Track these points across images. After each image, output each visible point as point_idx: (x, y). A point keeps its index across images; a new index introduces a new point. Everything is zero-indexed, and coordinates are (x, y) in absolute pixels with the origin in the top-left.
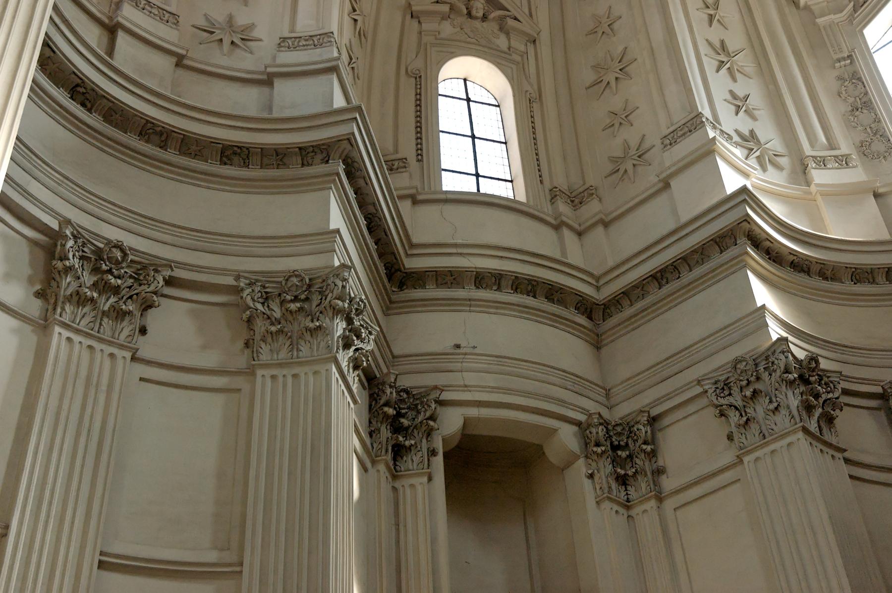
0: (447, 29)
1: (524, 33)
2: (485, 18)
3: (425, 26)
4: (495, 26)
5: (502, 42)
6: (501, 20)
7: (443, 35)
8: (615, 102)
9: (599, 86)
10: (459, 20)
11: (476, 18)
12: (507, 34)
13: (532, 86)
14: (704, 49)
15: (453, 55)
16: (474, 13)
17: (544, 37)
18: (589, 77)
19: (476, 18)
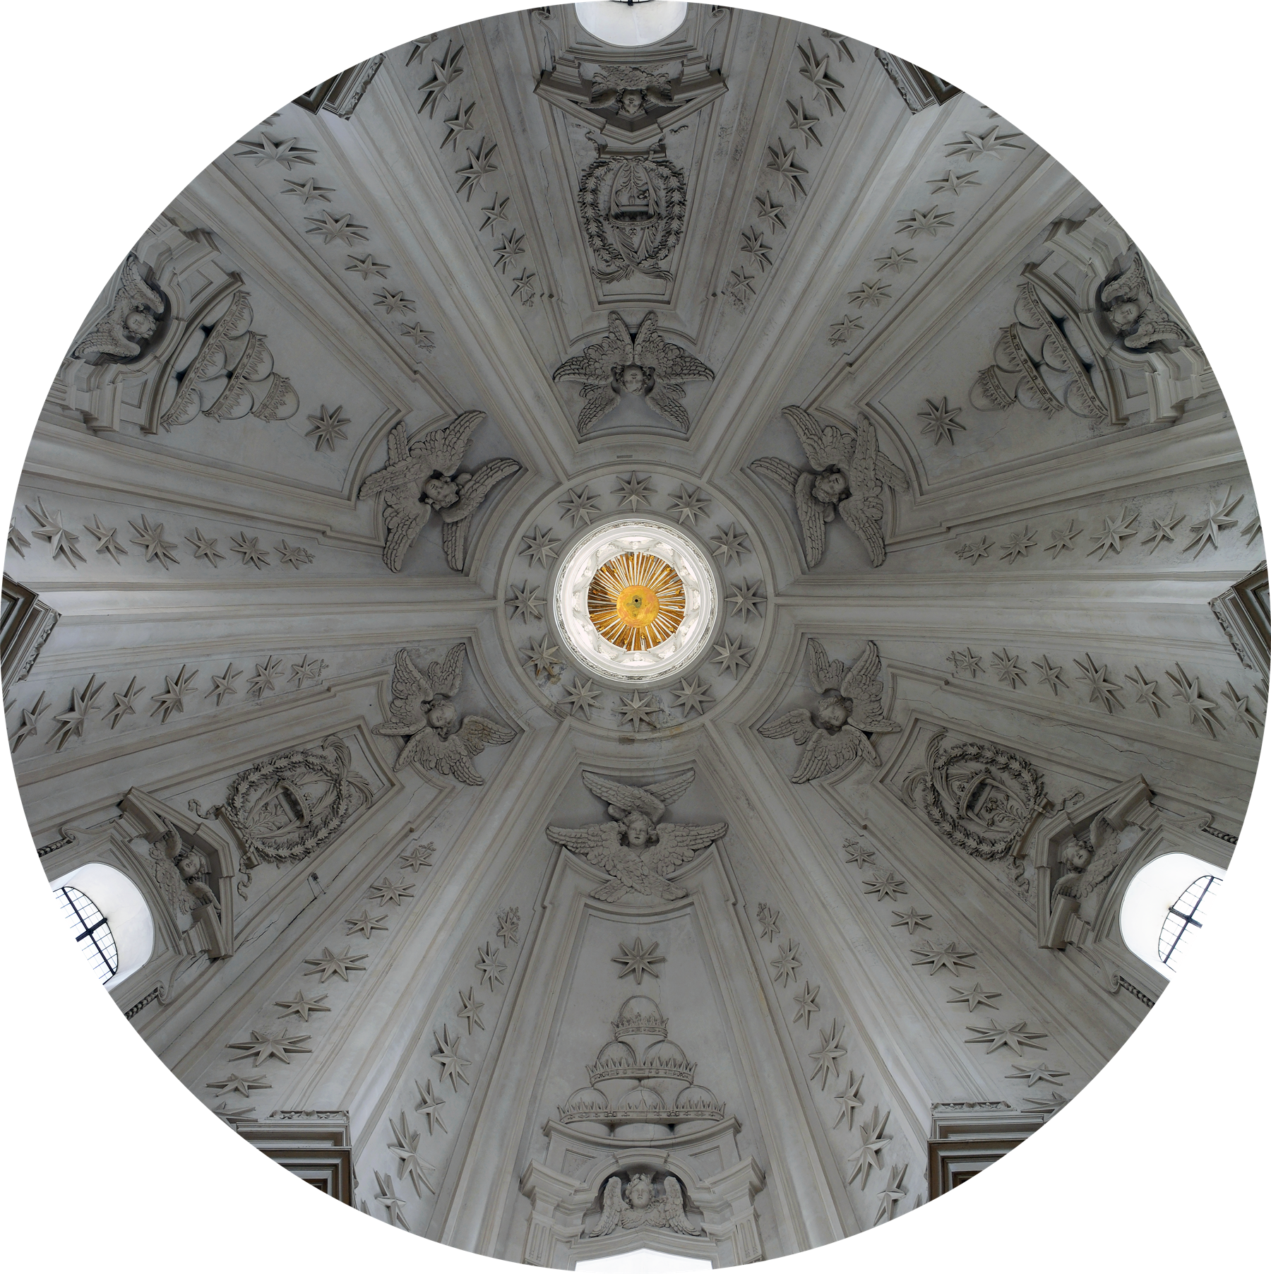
0: (142, 848)
1: (212, 938)
2: (189, 880)
3: (122, 821)
4: (191, 901)
5: (184, 921)
6: (205, 900)
7: (132, 846)
8: (247, 1070)
9: (247, 1050)
10: (161, 851)
11: (182, 871)
12: (196, 917)
13: (171, 986)
14: (390, 1111)
15: (122, 868)
16: (185, 863)
17: (231, 969)
18: (243, 1037)
19: (182, 871)
